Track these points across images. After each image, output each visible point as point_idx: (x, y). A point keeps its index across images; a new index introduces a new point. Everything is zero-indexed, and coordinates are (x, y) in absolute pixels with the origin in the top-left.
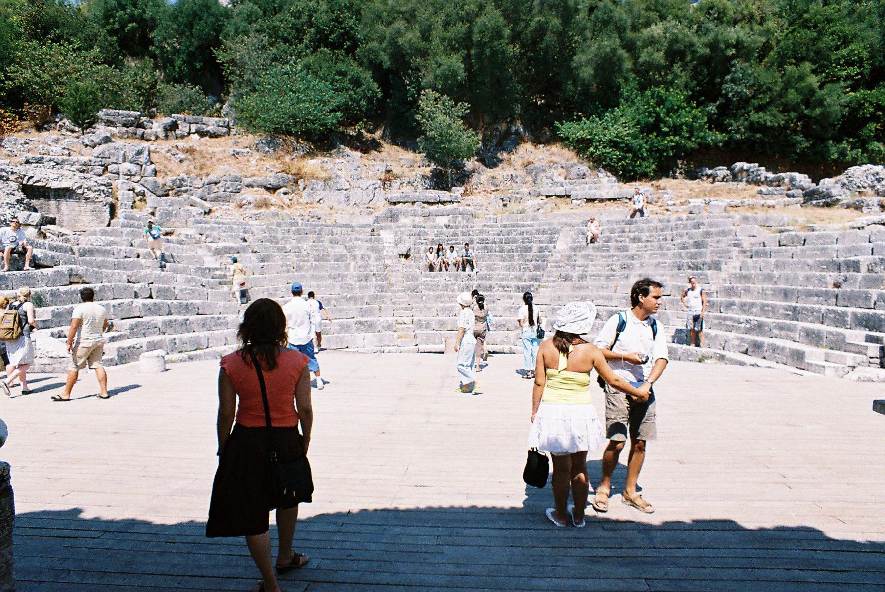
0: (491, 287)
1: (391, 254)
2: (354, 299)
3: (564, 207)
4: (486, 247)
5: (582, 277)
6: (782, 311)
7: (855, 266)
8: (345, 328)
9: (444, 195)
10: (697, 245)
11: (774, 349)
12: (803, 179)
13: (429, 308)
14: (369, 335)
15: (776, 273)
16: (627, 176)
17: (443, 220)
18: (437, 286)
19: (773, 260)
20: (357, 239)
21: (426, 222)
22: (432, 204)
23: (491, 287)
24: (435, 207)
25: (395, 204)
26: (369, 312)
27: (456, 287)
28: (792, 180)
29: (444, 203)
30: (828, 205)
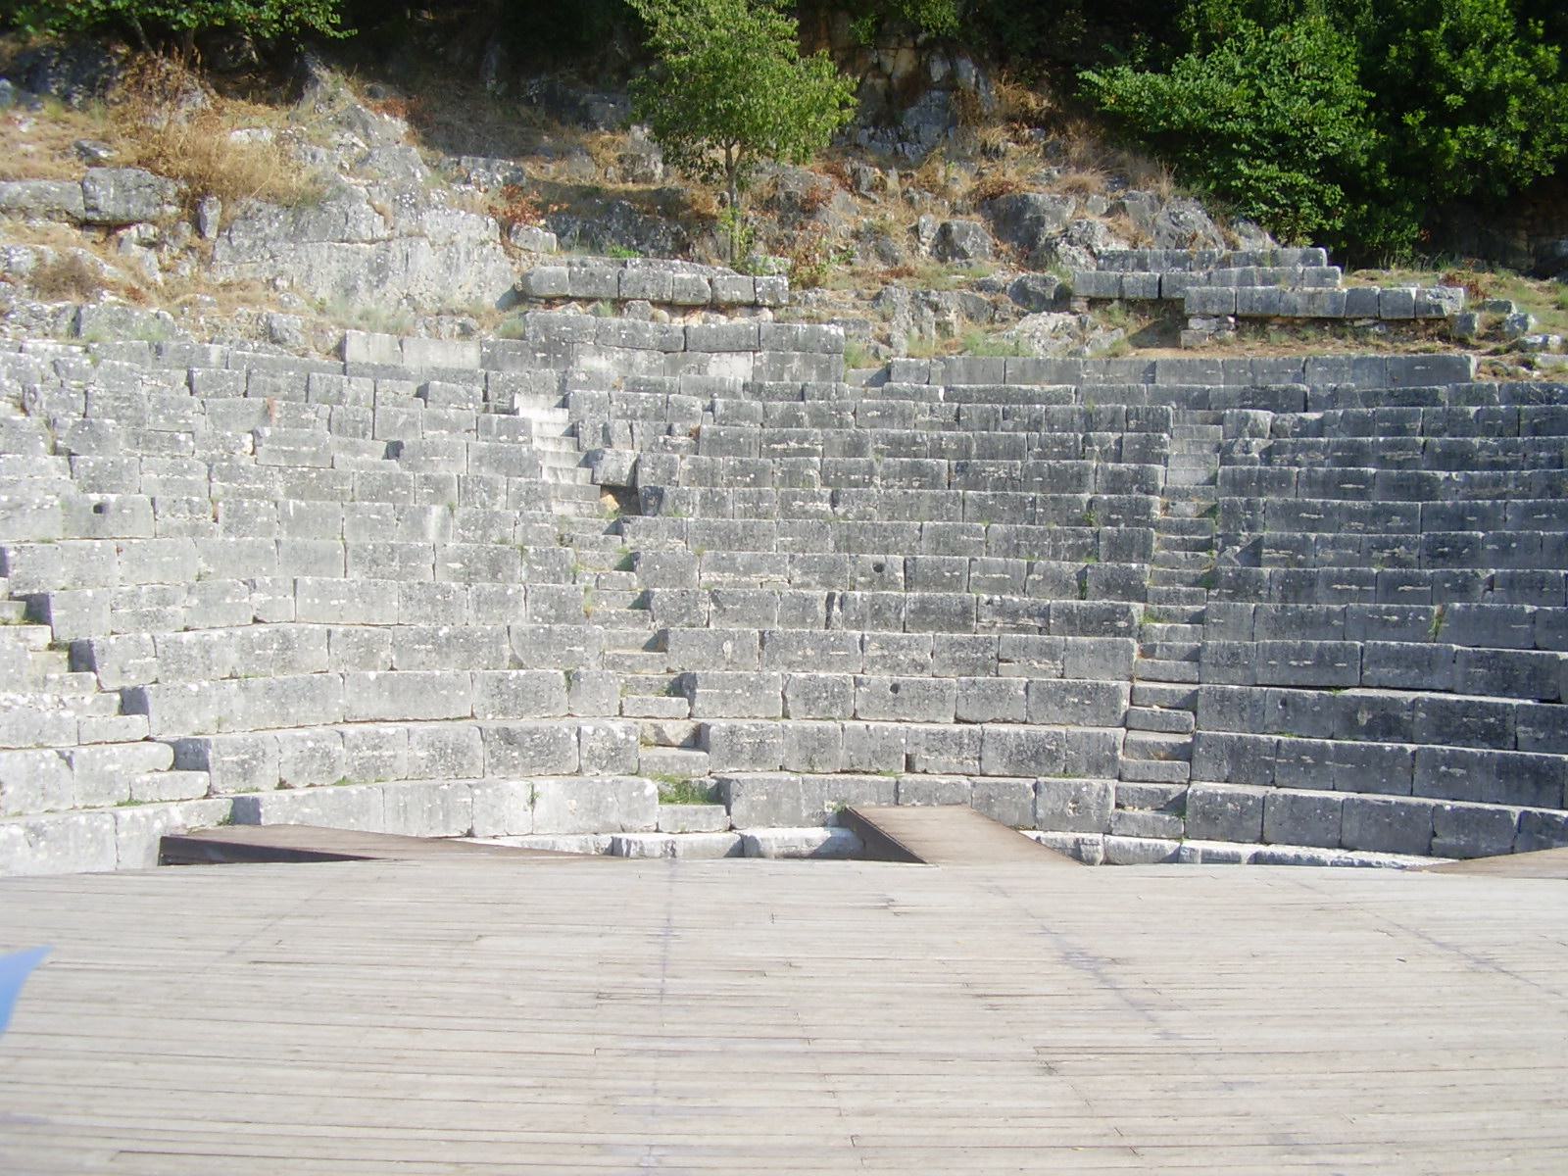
0: (965, 612)
1: (566, 481)
2: (466, 645)
4: (917, 470)
8: (450, 757)
13: (755, 687)
14: (550, 787)
17: (736, 369)
18: (764, 602)
20: (437, 422)
21: (674, 368)
22: (687, 309)
24: (695, 321)
26: (528, 697)
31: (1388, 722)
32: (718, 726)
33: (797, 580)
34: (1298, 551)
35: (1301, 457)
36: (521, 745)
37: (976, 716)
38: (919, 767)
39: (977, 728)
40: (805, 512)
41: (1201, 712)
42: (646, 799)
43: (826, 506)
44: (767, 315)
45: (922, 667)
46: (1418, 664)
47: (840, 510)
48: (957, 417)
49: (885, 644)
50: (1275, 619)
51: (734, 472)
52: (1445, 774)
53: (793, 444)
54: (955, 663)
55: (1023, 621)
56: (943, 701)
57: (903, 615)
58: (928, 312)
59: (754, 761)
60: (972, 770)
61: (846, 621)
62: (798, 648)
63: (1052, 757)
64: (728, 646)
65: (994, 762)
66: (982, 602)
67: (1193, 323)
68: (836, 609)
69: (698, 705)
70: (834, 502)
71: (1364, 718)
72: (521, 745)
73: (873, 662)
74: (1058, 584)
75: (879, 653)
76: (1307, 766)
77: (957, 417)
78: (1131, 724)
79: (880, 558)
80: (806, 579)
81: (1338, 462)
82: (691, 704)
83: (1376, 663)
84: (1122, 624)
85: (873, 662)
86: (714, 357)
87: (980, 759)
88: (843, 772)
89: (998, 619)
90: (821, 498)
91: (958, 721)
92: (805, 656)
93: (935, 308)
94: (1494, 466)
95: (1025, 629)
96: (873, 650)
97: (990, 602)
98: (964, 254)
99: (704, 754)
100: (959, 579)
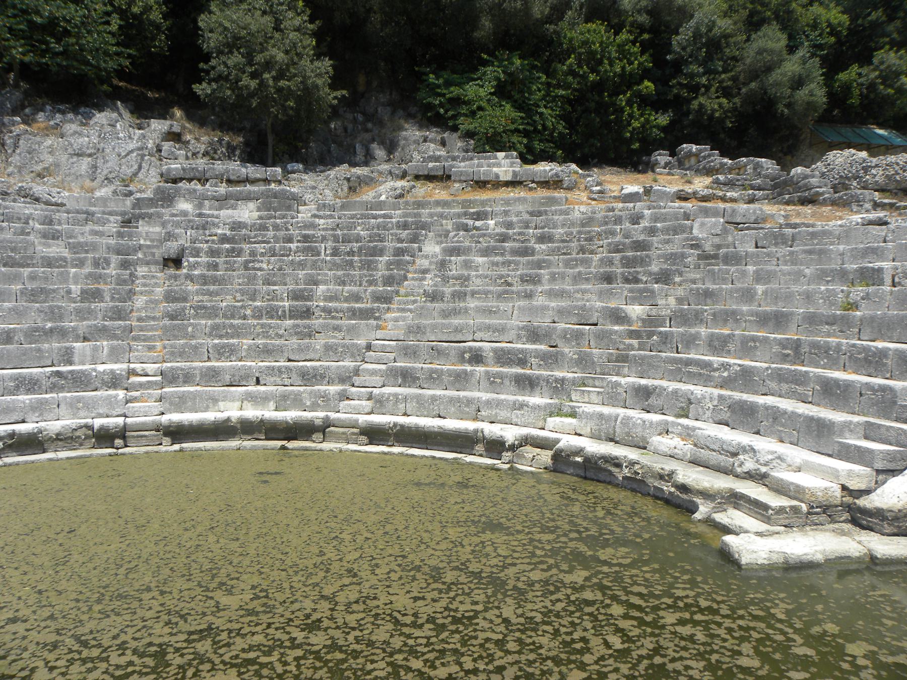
3: (439, 193)
5: (460, 296)
6: (776, 349)
7: (872, 277)
9: (253, 171)
10: (640, 246)
11: (776, 415)
12: (768, 165)
15: (760, 289)
16: (529, 157)
19: (751, 268)
21: (220, 209)
23: (308, 310)
25: (175, 181)
27: (248, 312)
28: (757, 166)
29: (253, 182)
30: (804, 202)
31: (477, 358)
34: (465, 280)
35: (481, 239)
37: (297, 358)
38: (262, 382)
44: (273, 186)
45: (281, 336)
46: (498, 331)
49: (263, 326)
51: (228, 250)
52: (493, 382)
54: (296, 333)
60: (286, 383)
61: (254, 317)
63: (323, 377)
64: (190, 329)
65: (296, 379)
71: (467, 356)
73: (258, 335)
76: (433, 378)
83: (480, 330)
85: (258, 335)
86: (239, 203)
90: (262, 262)
91: (290, 360)
92: (227, 332)
94: (563, 241)
95: (333, 318)
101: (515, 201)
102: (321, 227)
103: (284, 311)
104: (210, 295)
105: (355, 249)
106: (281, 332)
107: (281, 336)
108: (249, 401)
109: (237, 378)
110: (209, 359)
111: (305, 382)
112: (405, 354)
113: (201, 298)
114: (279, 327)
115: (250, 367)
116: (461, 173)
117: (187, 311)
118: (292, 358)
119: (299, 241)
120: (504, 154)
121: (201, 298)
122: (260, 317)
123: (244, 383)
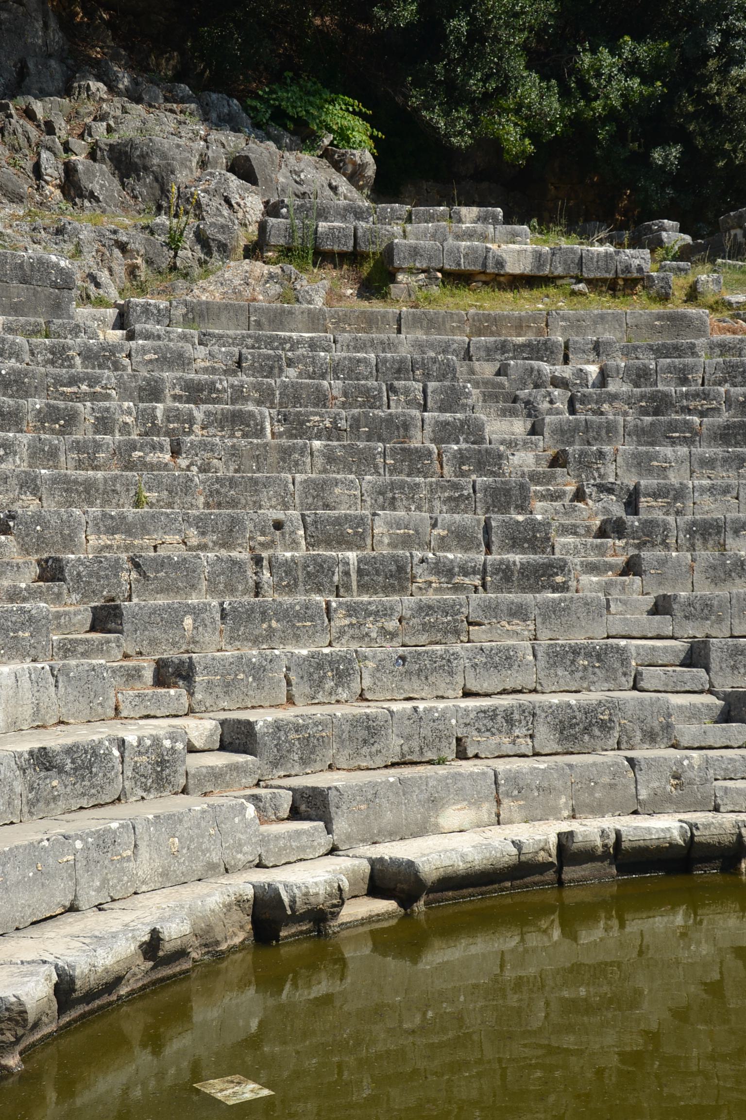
23: (401, 569)
32: (262, 719)
33: (194, 541)
34: (675, 499)
35: (606, 407)
36: (61, 770)
37: (486, 687)
39: (524, 698)
40: (145, 464)
41: (714, 665)
42: (248, 826)
43: (167, 457)
45: (393, 635)
47: (183, 462)
48: (239, 363)
49: (352, 610)
50: (714, 568)
53: (84, 387)
54: (426, 628)
55: (457, 579)
56: (451, 673)
57: (336, 578)
58: (117, 252)
59: (304, 762)
60: (524, 750)
62: (263, 621)
64: (188, 622)
65: (546, 738)
66: (416, 560)
67: (400, 277)
68: (266, 574)
69: (199, 696)
70: (176, 453)
72: (61, 770)
74: (460, 537)
75: (347, 622)
77: (239, 363)
78: (643, 684)
79: (279, 515)
80: (204, 540)
81: (644, 412)
82: (191, 694)
84: (559, 579)
85: (342, 632)
87: (532, 736)
88: (394, 765)
89: (433, 578)
91: (467, 694)
93: (123, 247)
95: (458, 588)
96: (341, 621)
97: (422, 561)
98: (92, 196)
99: (250, 758)
100: (362, 537)
101: (595, 323)
102: (200, 364)
103: (347, 573)
104: (129, 532)
105: (342, 424)
106: (392, 624)
107: (393, 635)
108: (515, 799)
109: (415, 744)
110: (291, 700)
111: (569, 746)
112: (734, 668)
113: (105, 540)
114: (387, 612)
115: (444, 712)
116: (415, 252)
117: (124, 575)
118: (473, 686)
119: (175, 398)
120: (475, 210)
121: (105, 540)
122: (291, 589)
123: (429, 755)
